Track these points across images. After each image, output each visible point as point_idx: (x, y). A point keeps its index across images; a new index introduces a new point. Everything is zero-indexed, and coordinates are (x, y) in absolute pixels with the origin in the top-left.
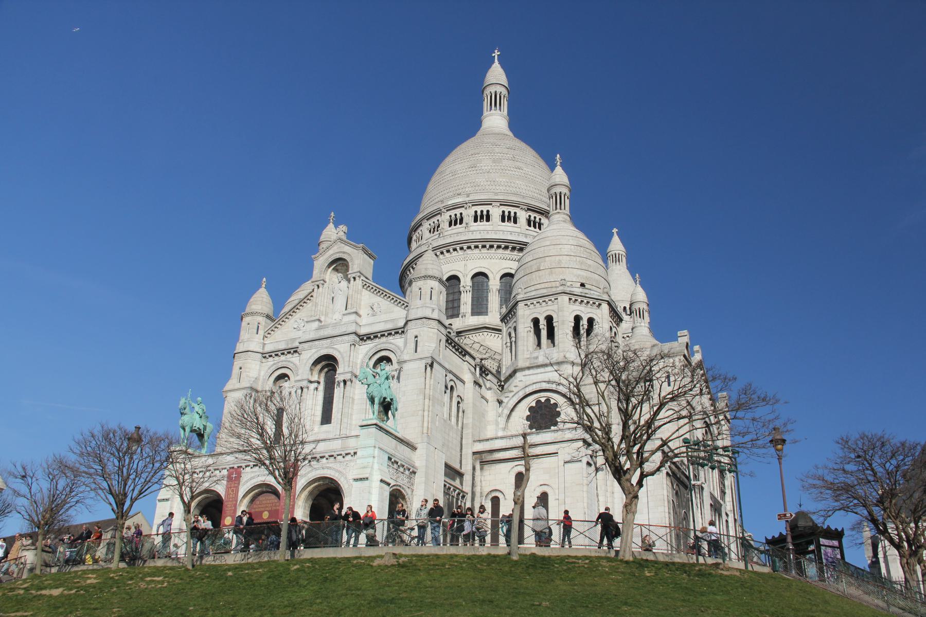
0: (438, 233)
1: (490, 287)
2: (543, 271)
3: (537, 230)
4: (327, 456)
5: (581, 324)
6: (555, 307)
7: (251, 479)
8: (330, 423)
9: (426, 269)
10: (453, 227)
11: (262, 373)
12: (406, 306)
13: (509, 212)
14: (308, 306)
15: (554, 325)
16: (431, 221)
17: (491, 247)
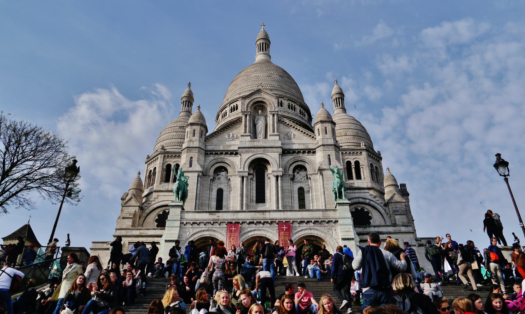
3: (304, 117)
4: (313, 221)
7: (248, 232)
11: (206, 164)
13: (292, 104)
14: (237, 126)
15: (361, 166)
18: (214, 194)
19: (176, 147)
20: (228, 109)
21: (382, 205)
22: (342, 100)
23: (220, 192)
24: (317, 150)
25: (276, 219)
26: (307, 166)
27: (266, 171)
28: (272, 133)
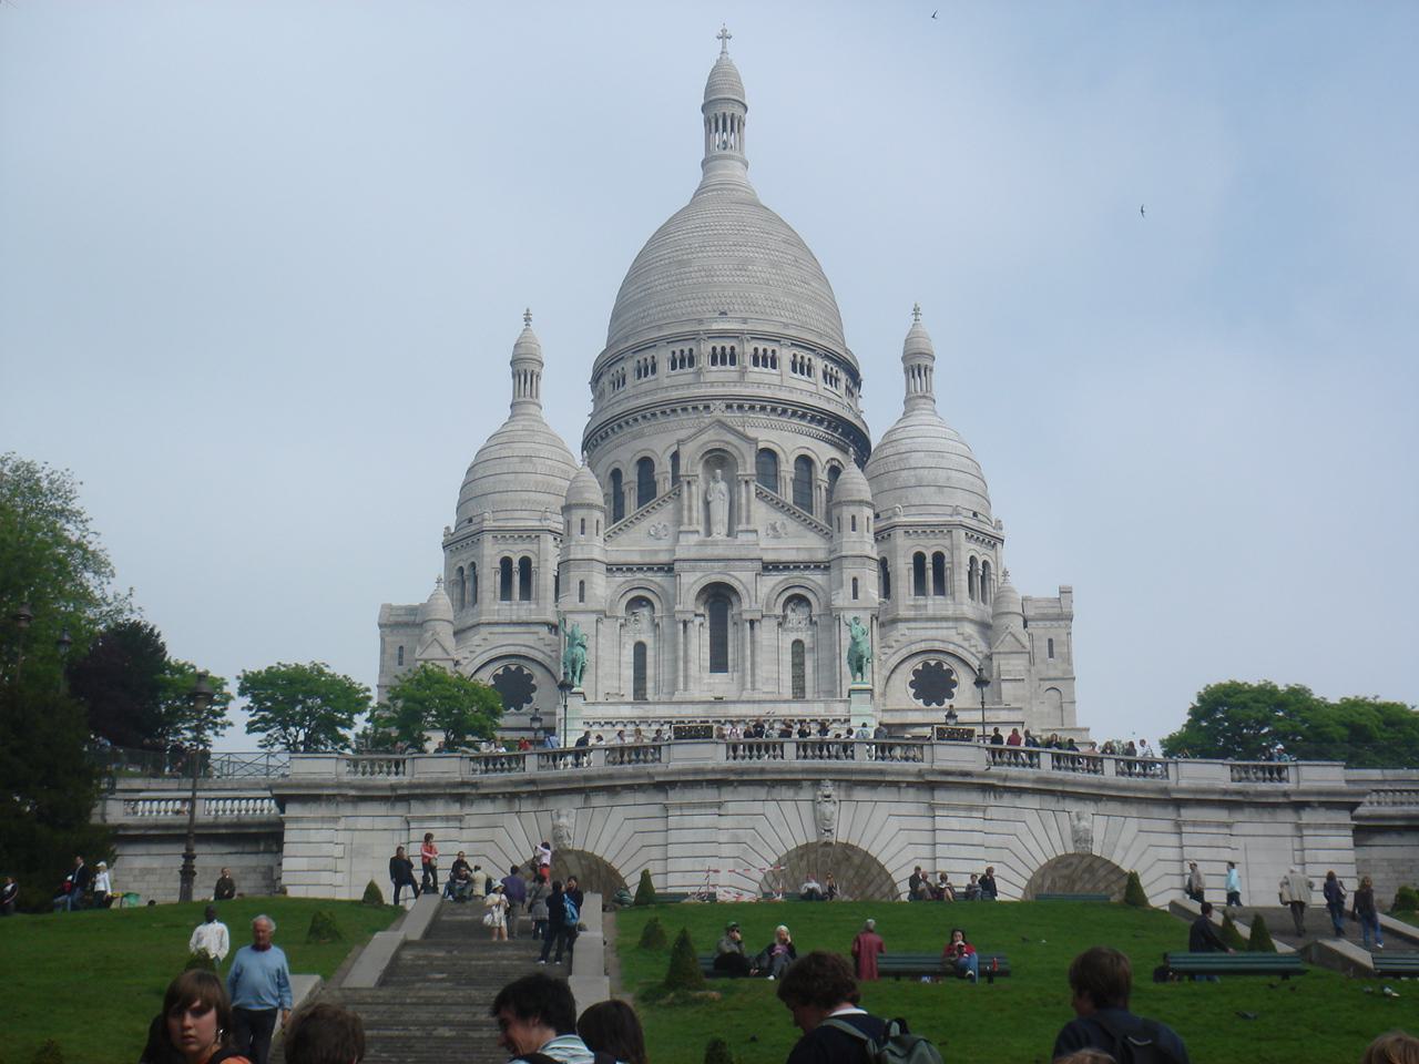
0: (691, 370)
1: (783, 474)
2: (927, 488)
3: (833, 389)
5: (974, 568)
6: (947, 542)
8: (727, 671)
9: (859, 491)
10: (719, 367)
11: (609, 592)
12: (828, 536)
13: (802, 357)
14: (671, 506)
15: (947, 566)
16: (677, 348)
17: (784, 411)
18: (628, 655)
19: (517, 515)
20: (629, 366)
21: (980, 656)
22: (928, 373)
23: (640, 649)
24: (832, 563)
25: (746, 717)
26: (810, 596)
27: (730, 607)
28: (741, 527)
